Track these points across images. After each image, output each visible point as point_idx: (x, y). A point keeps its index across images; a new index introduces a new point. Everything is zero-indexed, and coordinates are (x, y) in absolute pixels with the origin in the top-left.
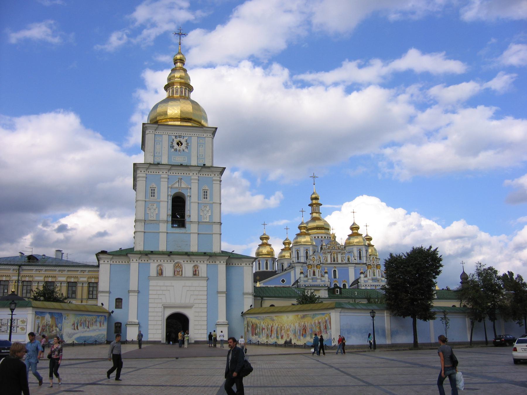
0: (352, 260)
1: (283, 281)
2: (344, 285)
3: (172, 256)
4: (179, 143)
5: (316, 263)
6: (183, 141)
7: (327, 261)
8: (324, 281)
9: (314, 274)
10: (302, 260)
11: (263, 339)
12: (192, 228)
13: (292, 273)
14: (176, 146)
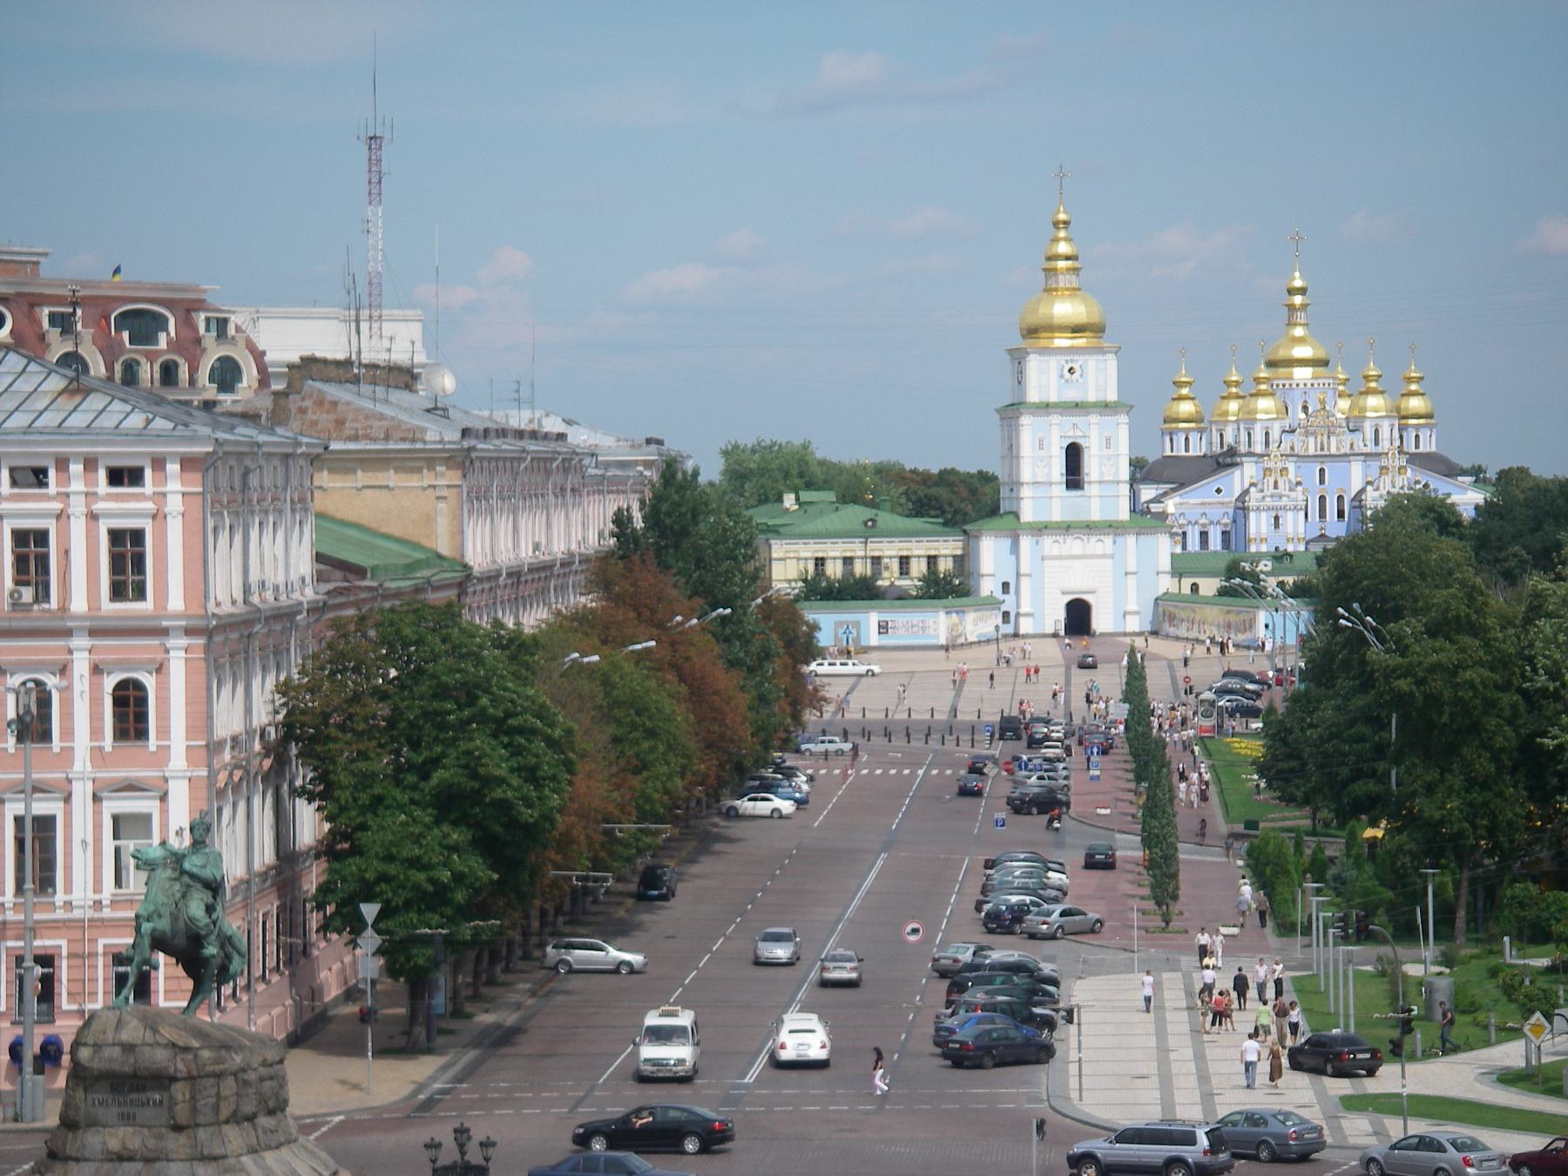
0: (1360, 447)
1: (1219, 491)
2: (1340, 498)
3: (1071, 531)
4: (1071, 370)
5: (1280, 465)
6: (1076, 366)
7: (1307, 449)
8: (1296, 500)
9: (1276, 486)
10: (1259, 448)
11: (1182, 632)
12: (1091, 490)
13: (1237, 473)
14: (1067, 375)
